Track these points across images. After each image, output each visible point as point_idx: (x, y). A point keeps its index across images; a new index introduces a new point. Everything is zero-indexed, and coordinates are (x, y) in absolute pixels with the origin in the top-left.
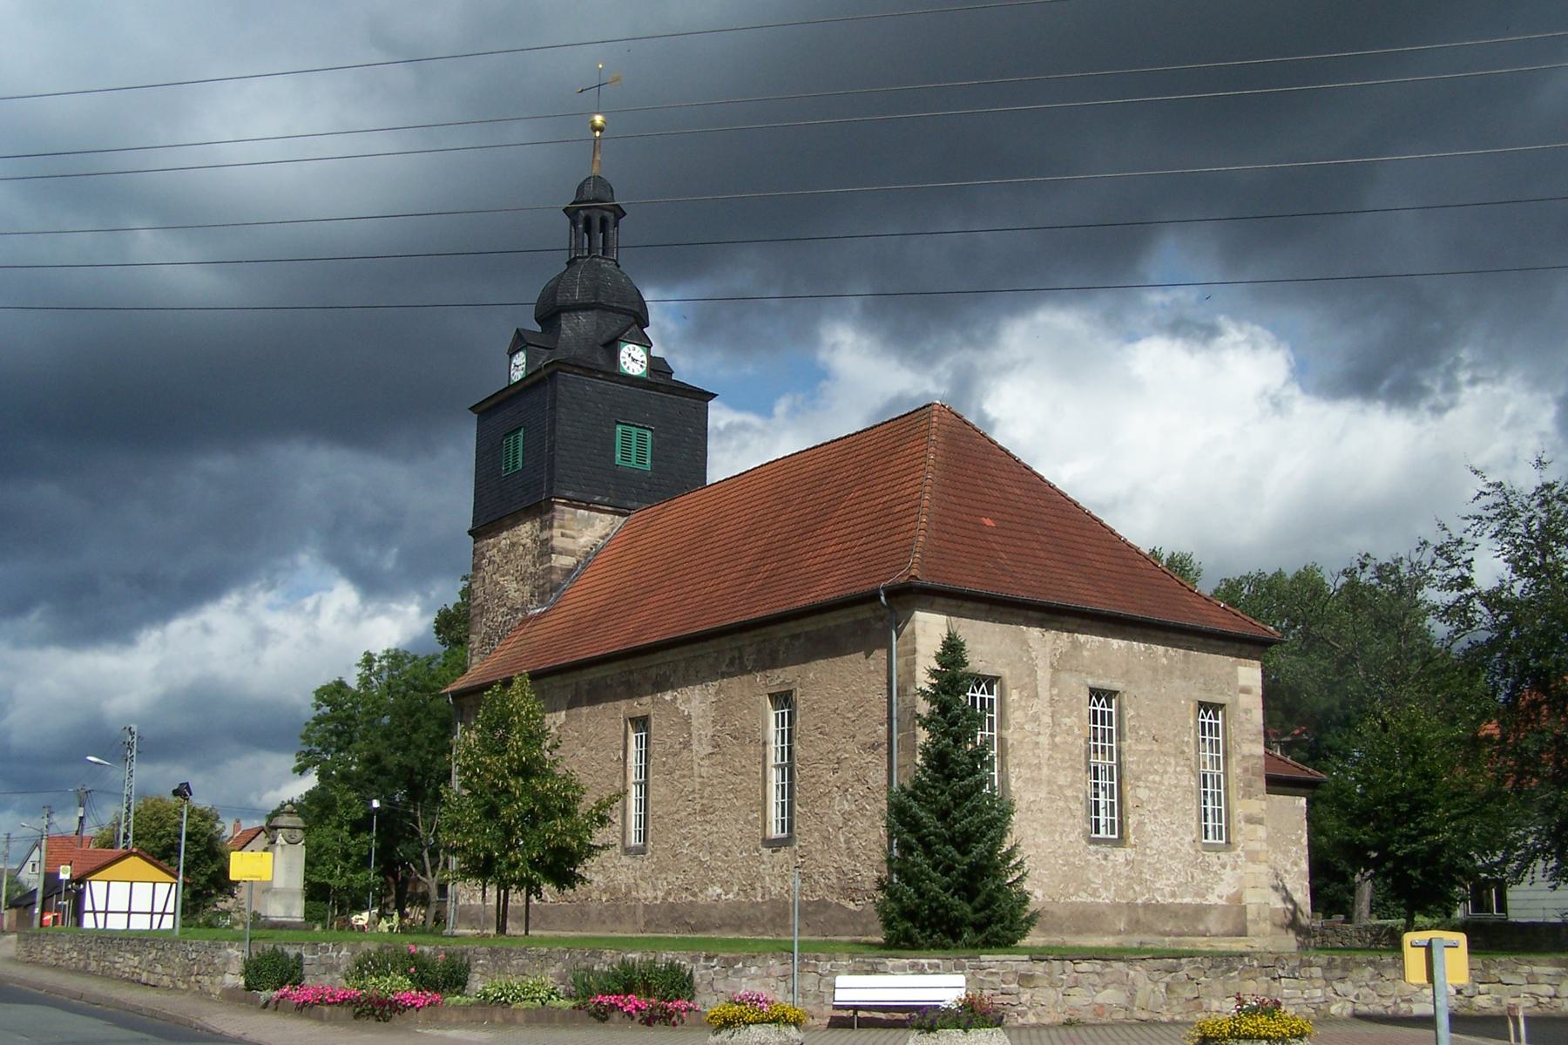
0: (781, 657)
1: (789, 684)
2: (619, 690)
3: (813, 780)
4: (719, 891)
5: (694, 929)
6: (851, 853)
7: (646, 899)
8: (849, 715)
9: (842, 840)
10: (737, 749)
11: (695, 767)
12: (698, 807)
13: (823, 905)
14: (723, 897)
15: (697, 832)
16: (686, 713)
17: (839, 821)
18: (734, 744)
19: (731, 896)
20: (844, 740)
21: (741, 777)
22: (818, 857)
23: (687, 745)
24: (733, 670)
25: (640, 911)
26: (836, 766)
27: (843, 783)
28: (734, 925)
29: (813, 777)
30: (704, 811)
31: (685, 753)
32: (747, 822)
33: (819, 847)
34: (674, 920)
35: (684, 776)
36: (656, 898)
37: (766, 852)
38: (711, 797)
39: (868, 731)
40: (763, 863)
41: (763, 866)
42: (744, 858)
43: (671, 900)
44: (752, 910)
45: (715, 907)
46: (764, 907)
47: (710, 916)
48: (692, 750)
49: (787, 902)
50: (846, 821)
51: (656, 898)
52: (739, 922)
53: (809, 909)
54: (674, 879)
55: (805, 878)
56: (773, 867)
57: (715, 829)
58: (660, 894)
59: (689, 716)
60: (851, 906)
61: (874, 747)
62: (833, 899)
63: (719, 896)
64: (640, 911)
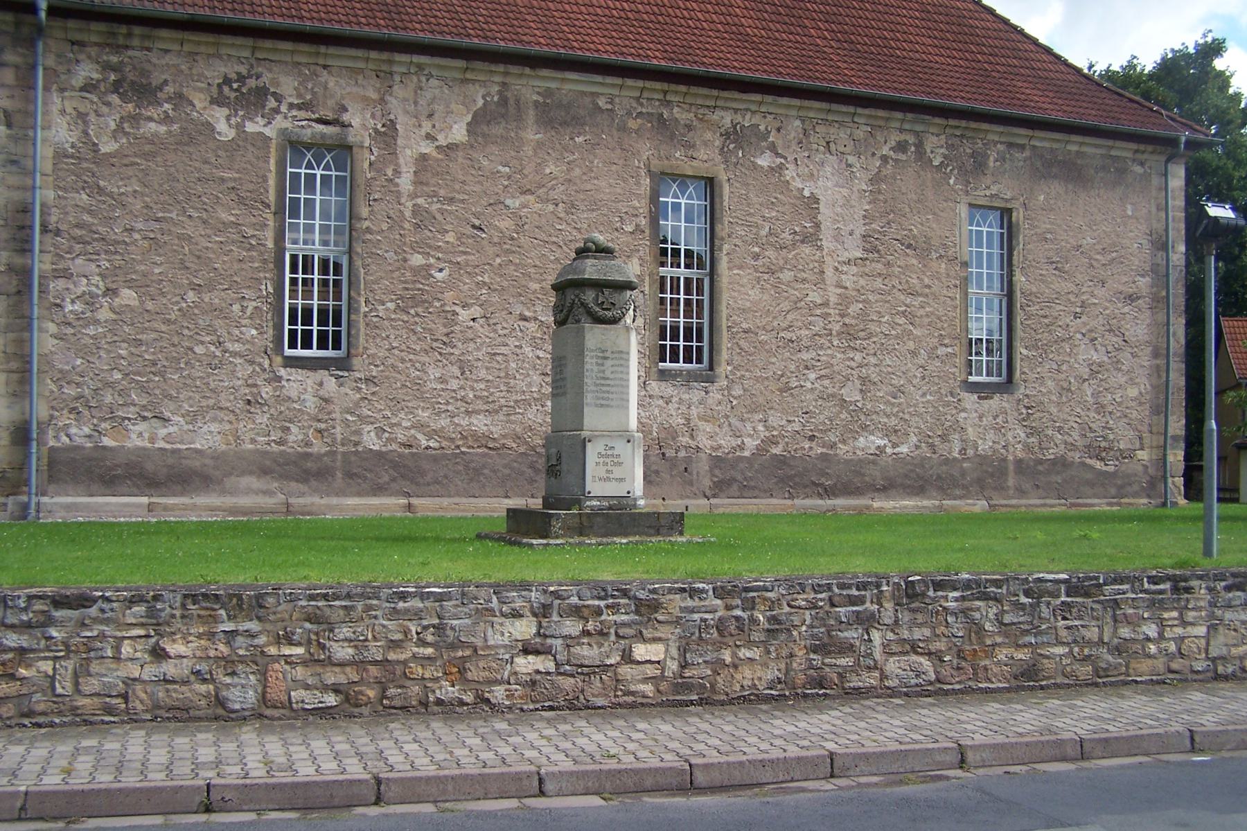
0: (991, 164)
1: (1007, 201)
2: (632, 124)
3: (1046, 321)
4: (881, 442)
5: (829, 492)
6: (1100, 408)
7: (714, 449)
8: (1098, 257)
9: (1089, 393)
10: (914, 261)
11: (829, 272)
12: (836, 328)
13: (1061, 464)
14: (889, 450)
15: (834, 361)
16: (806, 193)
17: (1085, 372)
18: (908, 255)
19: (904, 449)
20: (1091, 283)
21: (921, 299)
22: (1054, 410)
23: (811, 238)
24: (904, 157)
25: (702, 466)
26: (1078, 310)
27: (1091, 331)
28: (909, 486)
29: (1045, 317)
30: (848, 333)
31: (806, 250)
32: (932, 355)
33: (1054, 398)
34: (782, 480)
35: (804, 280)
36: (741, 447)
37: (970, 399)
38: (862, 316)
39: (1125, 279)
40: (964, 410)
41: (963, 415)
42: (928, 402)
43: (776, 450)
44: (944, 468)
45: (874, 463)
46: (965, 465)
47: (864, 475)
48: (820, 248)
49: (1005, 460)
50: (1093, 373)
51: (741, 447)
52: (921, 483)
53: (1040, 468)
54: (784, 422)
55: (1032, 432)
56: (980, 418)
57: (873, 360)
58: (751, 444)
59: (814, 199)
60: (1098, 465)
61: (1131, 298)
62: (1076, 456)
63: (881, 449)
64: (702, 466)
